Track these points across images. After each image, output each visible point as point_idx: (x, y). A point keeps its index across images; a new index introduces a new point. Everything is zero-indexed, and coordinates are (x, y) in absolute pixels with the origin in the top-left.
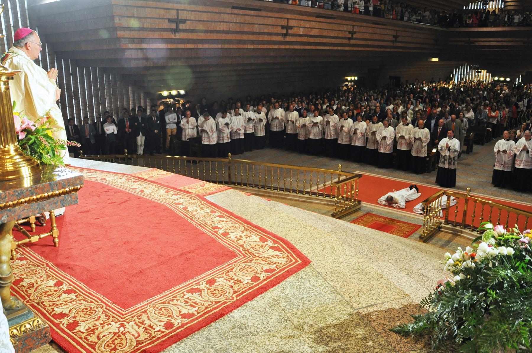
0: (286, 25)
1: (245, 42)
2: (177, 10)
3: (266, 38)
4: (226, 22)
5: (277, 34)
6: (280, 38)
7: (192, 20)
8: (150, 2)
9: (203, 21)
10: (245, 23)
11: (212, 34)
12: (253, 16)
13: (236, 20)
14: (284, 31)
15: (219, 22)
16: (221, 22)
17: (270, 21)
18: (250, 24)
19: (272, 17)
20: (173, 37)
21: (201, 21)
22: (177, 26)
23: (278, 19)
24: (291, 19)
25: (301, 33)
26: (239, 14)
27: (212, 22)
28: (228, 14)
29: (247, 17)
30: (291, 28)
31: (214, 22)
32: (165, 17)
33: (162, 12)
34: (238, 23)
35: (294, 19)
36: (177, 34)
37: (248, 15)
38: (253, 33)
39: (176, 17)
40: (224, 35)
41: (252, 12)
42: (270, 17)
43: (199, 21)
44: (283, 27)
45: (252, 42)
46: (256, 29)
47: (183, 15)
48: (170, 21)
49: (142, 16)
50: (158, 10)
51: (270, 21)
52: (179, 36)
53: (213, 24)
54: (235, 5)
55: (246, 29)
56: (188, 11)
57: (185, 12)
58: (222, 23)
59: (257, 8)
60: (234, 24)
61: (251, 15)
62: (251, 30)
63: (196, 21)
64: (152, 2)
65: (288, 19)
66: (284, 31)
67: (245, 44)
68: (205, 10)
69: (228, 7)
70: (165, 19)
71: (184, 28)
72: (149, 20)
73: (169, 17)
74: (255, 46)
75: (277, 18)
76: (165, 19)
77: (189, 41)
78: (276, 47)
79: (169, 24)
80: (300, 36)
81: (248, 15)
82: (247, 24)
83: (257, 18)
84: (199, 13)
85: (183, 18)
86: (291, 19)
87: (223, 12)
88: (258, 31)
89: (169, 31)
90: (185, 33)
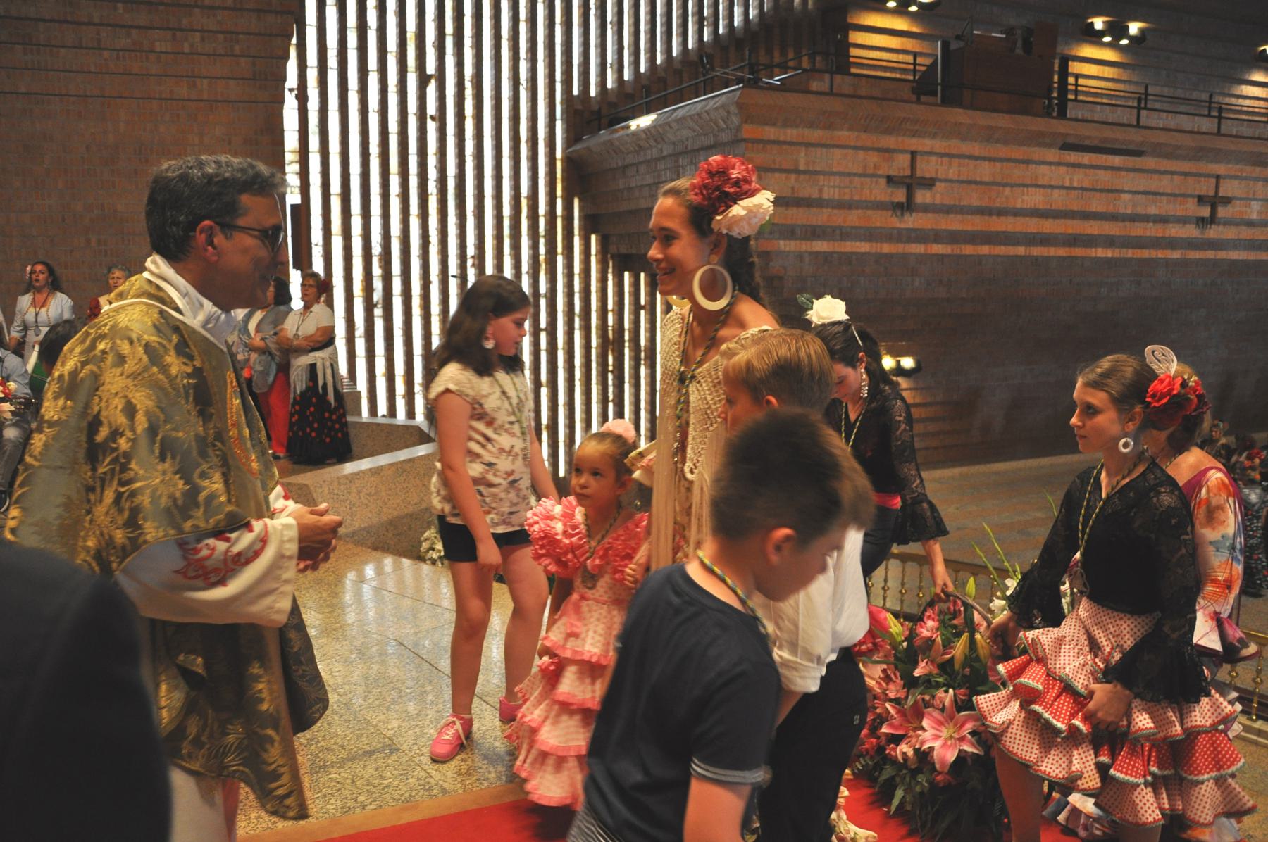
0: (1212, 193)
1: (1090, 241)
2: (913, 154)
3: (1152, 230)
4: (1043, 187)
5: (1183, 220)
6: (1191, 231)
7: (951, 181)
8: (840, 133)
9: (981, 183)
10: (1096, 190)
11: (1003, 219)
12: (1119, 169)
13: (1071, 179)
14: (1205, 212)
15: (1024, 185)
16: (1027, 186)
17: (1165, 184)
19: (1173, 173)
20: (898, 225)
21: (976, 183)
22: (910, 196)
23: (1191, 180)
24: (1226, 177)
25: (1254, 216)
26: (1079, 166)
28: (1050, 164)
29: (1101, 172)
30: (1227, 201)
31: (1012, 186)
32: (880, 172)
33: (873, 158)
34: (1075, 188)
35: (1236, 177)
36: (907, 217)
38: (1114, 217)
39: (908, 173)
40: (1035, 220)
41: (1117, 160)
42: (1166, 172)
43: (969, 182)
44: (1201, 199)
45: (1110, 242)
46: (1125, 204)
47: (927, 168)
49: (818, 169)
50: (861, 152)
51: (1165, 184)
52: (911, 221)
53: (1008, 190)
54: (1071, 140)
56: (942, 155)
57: (933, 158)
58: (1032, 190)
59: (1131, 147)
60: (1064, 192)
61: (1113, 168)
62: (1111, 209)
63: (962, 182)
64: (846, 133)
65: (1218, 177)
66: (1205, 212)
67: (1091, 247)
68: (987, 155)
69: (1050, 146)
70: (880, 176)
71: (928, 200)
72: (838, 179)
73: (891, 173)
74: (1117, 250)
75: (1186, 174)
76: (880, 176)
77: (937, 237)
78: (1176, 255)
79: (890, 190)
80: (1250, 224)
81: (1106, 168)
82: (1101, 191)
83: (1132, 175)
84: (972, 163)
85: (928, 176)
86: (1226, 177)
87: (1036, 157)
88: (1129, 211)
89: (888, 210)
90: (930, 215)
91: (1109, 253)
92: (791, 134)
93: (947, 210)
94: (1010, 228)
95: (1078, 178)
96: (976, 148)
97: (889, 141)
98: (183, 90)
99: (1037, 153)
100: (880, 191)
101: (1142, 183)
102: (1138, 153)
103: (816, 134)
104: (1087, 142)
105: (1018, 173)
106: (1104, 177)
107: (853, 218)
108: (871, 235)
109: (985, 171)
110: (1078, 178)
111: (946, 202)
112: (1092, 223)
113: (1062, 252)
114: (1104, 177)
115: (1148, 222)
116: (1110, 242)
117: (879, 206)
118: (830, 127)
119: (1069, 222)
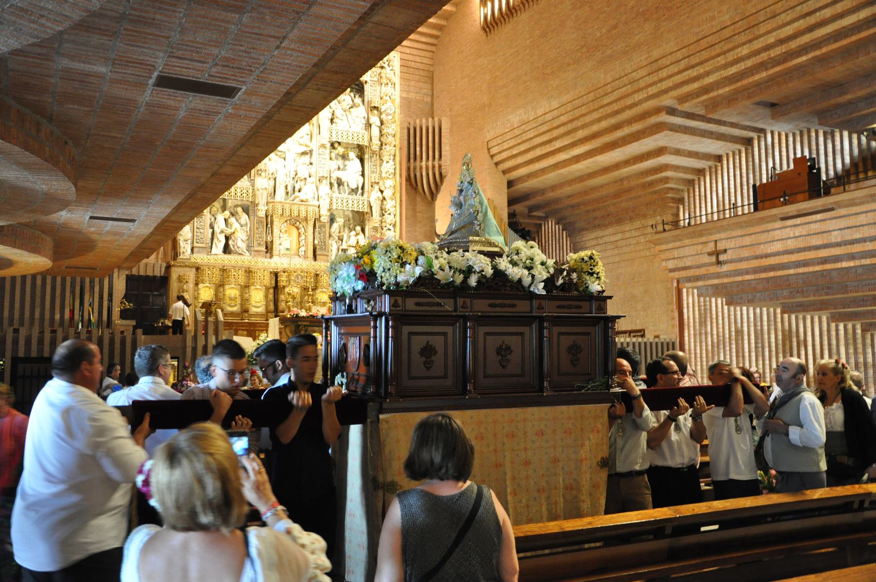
1: (837, 259)
2: (716, 241)
11: (768, 259)
12: (825, 220)
18: (818, 233)
27: (760, 244)
33: (700, 247)
37: (816, 222)
41: (819, 217)
45: (852, 257)
46: (836, 237)
47: (721, 246)
48: (710, 254)
52: (725, 268)
53: (762, 246)
55: (816, 241)
68: (743, 233)
69: (774, 221)
81: (816, 222)
87: (769, 228)
91: (852, 264)
92: (670, 246)
93: (741, 260)
94: (773, 263)
95: (797, 232)
96: (739, 232)
97: (704, 239)
98: (648, 254)
99: (770, 226)
100: (707, 259)
101: (843, 223)
102: (832, 209)
103: (678, 244)
104: (791, 214)
105: (763, 237)
106: (815, 227)
107: (702, 271)
108: (718, 276)
109: (747, 241)
110: (797, 232)
111: (734, 257)
112: (822, 250)
113: (818, 268)
114: (815, 227)
115: (865, 241)
116: (852, 257)
117: (711, 264)
118: (680, 240)
119: (806, 253)
